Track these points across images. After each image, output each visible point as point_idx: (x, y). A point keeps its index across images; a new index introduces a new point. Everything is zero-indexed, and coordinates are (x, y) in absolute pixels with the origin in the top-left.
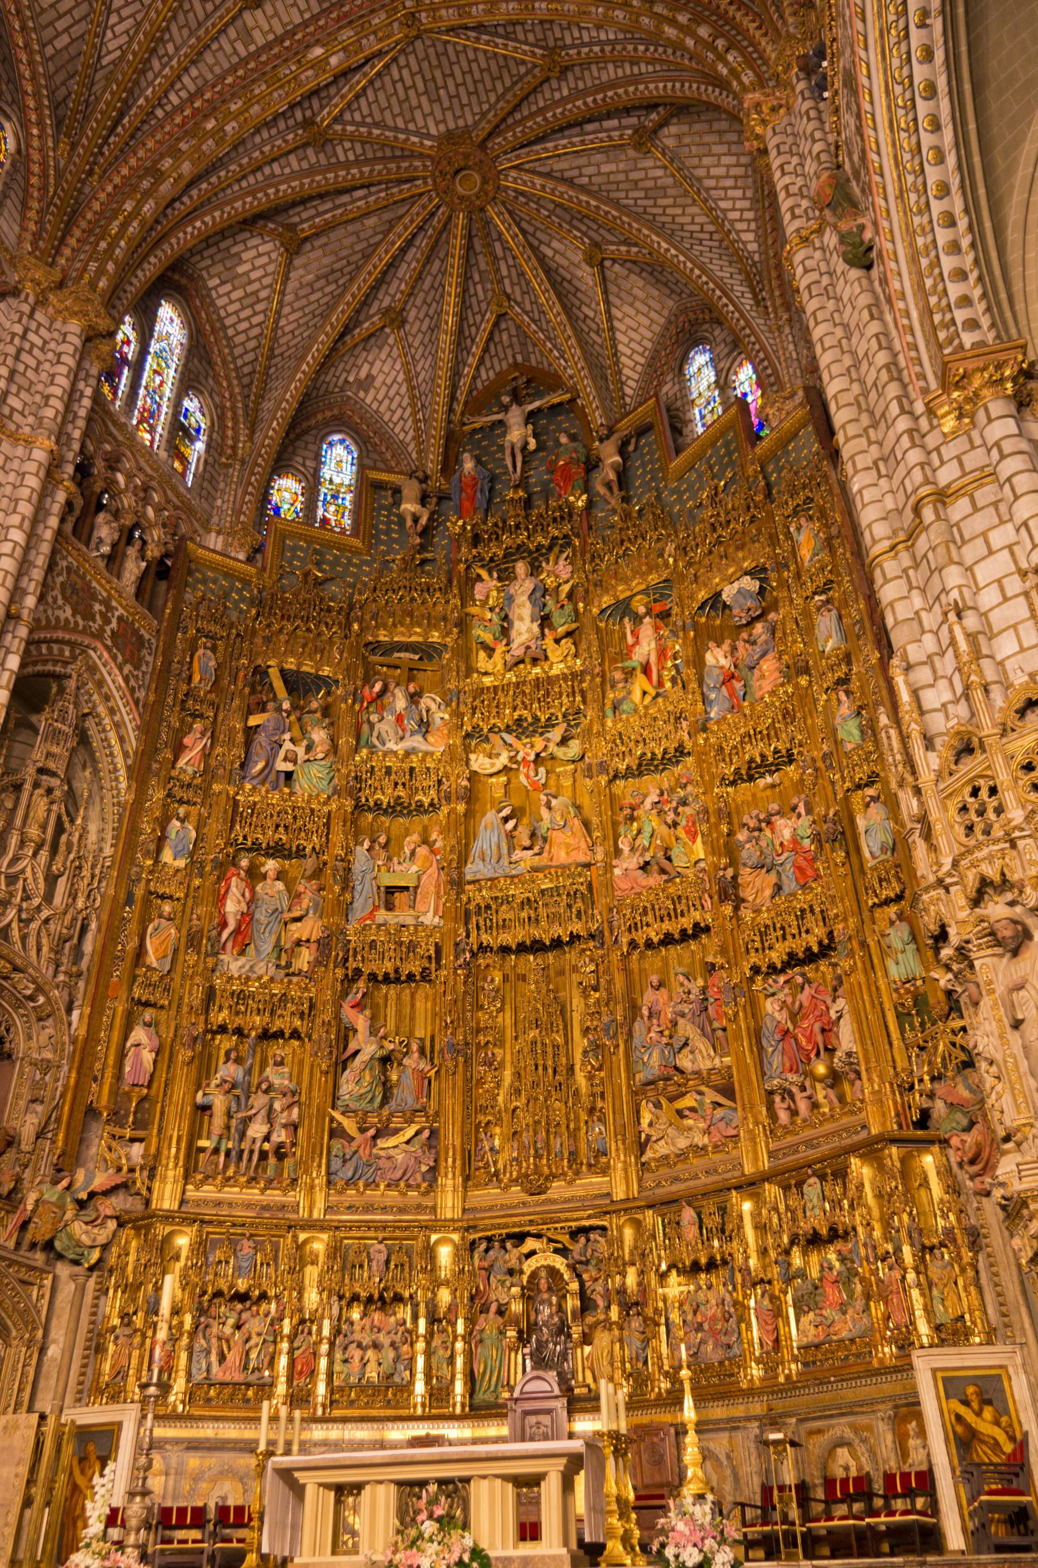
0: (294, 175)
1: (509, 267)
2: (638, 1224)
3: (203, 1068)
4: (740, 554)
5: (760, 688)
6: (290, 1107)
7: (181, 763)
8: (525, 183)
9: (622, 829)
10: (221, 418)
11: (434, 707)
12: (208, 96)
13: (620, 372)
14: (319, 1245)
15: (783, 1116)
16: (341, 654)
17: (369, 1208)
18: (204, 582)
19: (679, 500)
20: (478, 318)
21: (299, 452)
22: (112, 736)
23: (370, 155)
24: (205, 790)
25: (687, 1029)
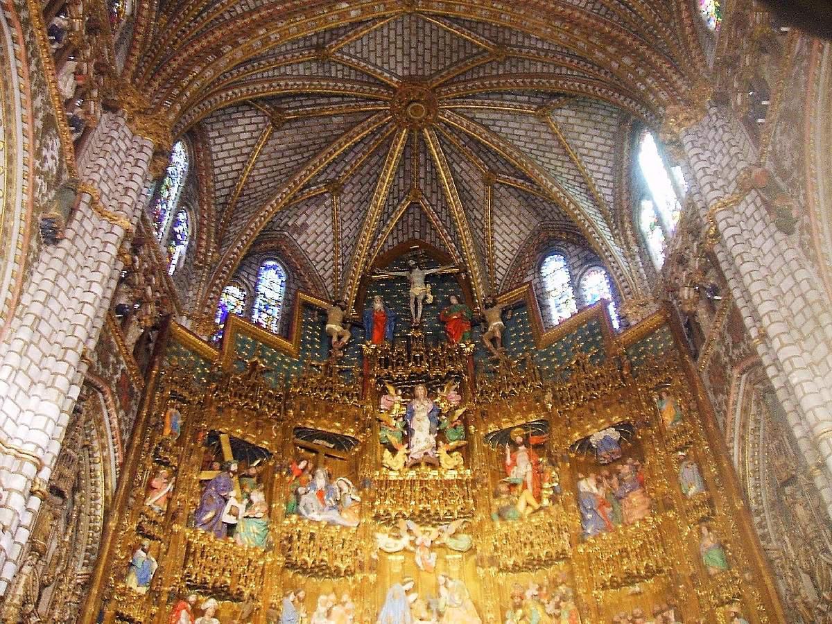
0: (299, 77)
1: (426, 172)
4: (608, 410)
5: (630, 515)
7: (149, 502)
8: (455, 121)
9: (509, 614)
10: (200, 231)
11: (345, 488)
12: (263, 13)
13: (494, 261)
16: (277, 431)
18: (178, 354)
19: (548, 362)
20: (396, 201)
21: (245, 268)
22: (99, 467)
23: (353, 77)
24: (166, 527)
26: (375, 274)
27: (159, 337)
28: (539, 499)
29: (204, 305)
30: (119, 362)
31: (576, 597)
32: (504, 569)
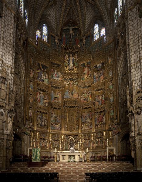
2: (81, 135)
3: (37, 116)
6: (46, 121)
9: (82, 95)
14: (51, 135)
15: (96, 127)
17: (55, 132)
25: (88, 118)
26: (63, 28)
27: (27, 42)
28: (88, 76)
29: (33, 35)
30: (21, 48)
31: (91, 92)
32: (82, 88)
